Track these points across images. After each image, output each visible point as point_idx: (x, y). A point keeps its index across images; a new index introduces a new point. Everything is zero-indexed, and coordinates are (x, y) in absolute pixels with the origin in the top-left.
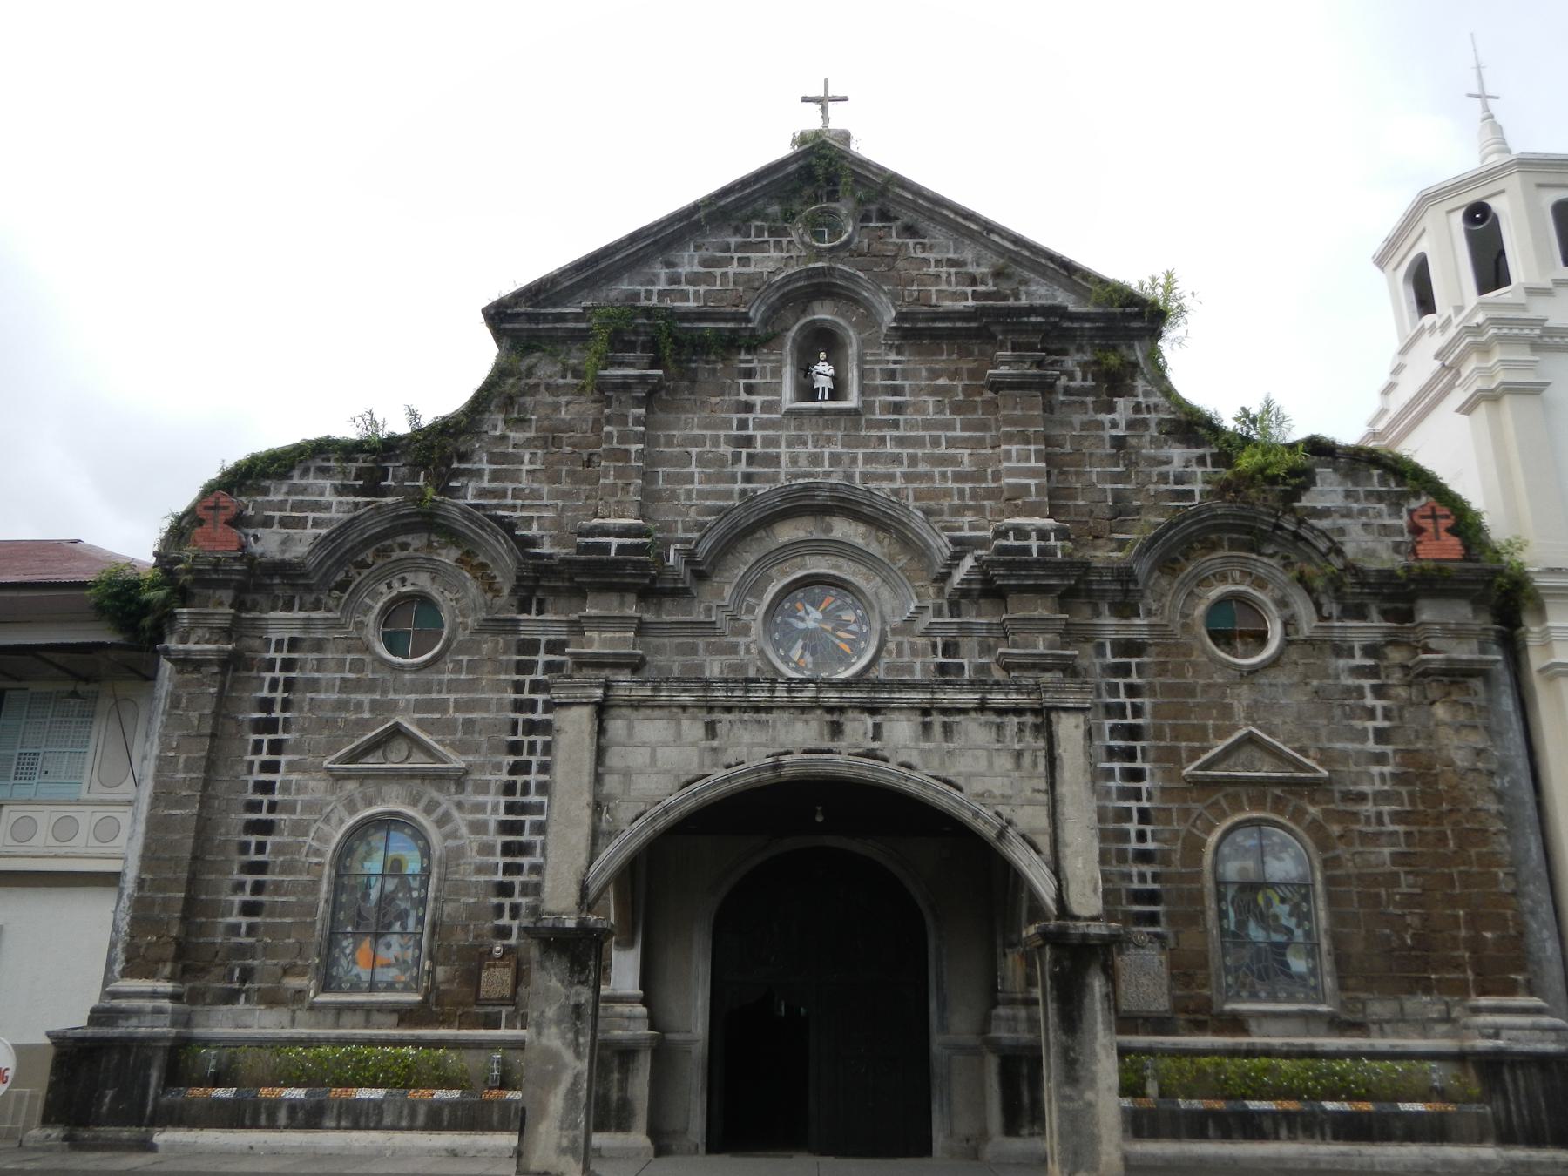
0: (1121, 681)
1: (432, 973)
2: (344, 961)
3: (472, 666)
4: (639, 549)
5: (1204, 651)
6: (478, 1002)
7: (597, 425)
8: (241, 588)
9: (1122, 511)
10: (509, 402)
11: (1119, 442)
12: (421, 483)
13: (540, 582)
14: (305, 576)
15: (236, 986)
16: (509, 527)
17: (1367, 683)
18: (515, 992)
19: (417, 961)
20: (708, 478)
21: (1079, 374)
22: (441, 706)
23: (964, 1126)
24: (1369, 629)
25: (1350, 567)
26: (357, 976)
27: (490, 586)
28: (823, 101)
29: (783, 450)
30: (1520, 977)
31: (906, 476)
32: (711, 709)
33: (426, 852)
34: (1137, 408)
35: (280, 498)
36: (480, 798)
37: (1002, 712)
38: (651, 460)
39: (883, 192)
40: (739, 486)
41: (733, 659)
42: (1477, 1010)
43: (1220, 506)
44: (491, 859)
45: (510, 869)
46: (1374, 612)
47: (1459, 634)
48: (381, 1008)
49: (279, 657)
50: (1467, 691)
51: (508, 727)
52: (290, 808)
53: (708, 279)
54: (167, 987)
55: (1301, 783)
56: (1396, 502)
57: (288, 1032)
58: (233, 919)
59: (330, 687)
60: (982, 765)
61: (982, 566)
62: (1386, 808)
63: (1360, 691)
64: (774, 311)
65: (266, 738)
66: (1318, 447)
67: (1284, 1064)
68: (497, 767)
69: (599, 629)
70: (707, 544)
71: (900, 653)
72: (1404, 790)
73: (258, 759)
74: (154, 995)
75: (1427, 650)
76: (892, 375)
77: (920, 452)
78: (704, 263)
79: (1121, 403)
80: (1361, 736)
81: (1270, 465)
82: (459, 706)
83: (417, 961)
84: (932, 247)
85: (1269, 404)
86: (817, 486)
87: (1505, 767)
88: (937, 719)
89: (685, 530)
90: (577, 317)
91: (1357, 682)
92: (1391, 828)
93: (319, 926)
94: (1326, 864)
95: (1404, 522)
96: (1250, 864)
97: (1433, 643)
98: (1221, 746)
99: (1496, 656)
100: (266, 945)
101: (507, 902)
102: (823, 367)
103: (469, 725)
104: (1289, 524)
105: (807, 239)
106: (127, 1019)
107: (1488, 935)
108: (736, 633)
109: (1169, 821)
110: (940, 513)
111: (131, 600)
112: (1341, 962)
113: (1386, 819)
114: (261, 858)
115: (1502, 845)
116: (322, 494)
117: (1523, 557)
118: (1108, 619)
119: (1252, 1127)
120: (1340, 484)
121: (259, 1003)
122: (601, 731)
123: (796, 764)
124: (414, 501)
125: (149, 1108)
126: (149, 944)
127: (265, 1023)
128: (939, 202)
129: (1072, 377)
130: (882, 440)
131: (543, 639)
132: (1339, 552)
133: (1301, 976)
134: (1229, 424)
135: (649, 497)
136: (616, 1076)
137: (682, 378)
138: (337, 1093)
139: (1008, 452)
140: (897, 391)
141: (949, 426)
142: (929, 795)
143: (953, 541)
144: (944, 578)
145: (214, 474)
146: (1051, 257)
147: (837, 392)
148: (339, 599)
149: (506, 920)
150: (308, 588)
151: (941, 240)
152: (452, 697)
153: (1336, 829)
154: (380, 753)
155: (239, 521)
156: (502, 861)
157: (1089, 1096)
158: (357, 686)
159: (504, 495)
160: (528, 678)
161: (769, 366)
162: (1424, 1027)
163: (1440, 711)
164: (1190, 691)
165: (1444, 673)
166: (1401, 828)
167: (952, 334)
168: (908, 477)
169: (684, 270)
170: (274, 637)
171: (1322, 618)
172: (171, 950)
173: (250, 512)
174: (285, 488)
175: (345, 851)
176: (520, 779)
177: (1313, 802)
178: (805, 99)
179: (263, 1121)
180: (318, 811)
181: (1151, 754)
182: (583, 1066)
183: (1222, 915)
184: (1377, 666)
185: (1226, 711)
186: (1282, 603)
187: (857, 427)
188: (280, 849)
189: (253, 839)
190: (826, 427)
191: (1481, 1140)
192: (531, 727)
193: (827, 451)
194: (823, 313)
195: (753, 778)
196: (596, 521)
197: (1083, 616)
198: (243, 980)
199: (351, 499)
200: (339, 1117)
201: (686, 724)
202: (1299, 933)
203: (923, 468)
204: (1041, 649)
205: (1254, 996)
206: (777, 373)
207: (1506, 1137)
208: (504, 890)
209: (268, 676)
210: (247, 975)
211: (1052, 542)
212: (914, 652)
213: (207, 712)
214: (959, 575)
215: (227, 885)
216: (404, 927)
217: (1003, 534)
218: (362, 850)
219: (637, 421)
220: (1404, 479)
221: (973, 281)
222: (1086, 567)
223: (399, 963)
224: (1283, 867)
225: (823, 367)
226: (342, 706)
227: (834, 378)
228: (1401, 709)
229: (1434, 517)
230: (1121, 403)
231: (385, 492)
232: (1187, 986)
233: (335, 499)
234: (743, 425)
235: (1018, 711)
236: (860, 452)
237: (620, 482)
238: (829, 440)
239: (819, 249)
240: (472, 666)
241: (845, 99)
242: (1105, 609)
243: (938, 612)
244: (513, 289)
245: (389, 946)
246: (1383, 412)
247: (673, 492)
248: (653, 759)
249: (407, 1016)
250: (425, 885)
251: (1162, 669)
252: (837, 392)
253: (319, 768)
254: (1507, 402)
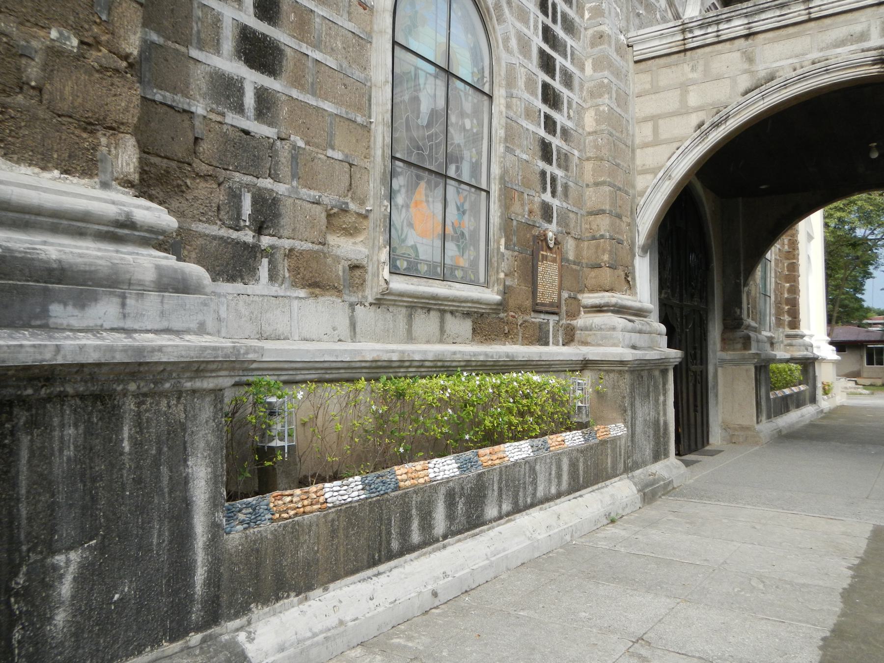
15: (247, 236)
26: (415, 248)
54: (151, 213)
74: (121, 231)
106: (82, 301)
121: (294, 285)
125: (200, 575)
126: (55, 52)
136: (662, 398)
198: (260, 230)
249: (486, 322)
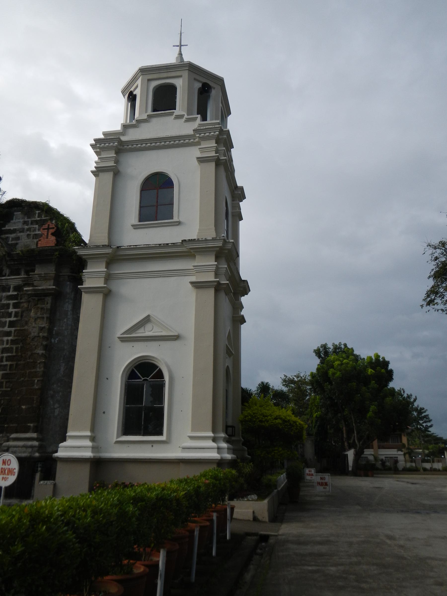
17: (11, 302)
30: (32, 425)
46: (23, 273)
47: (45, 278)
56: (41, 223)
62: (5, 355)
72: (14, 347)
91: (8, 302)
92: (5, 363)
99: (68, 289)
107: (24, 407)
113: (4, 359)
120: (23, 218)
165: (36, 295)
166: (9, 363)
184: (18, 294)
228: (23, 312)
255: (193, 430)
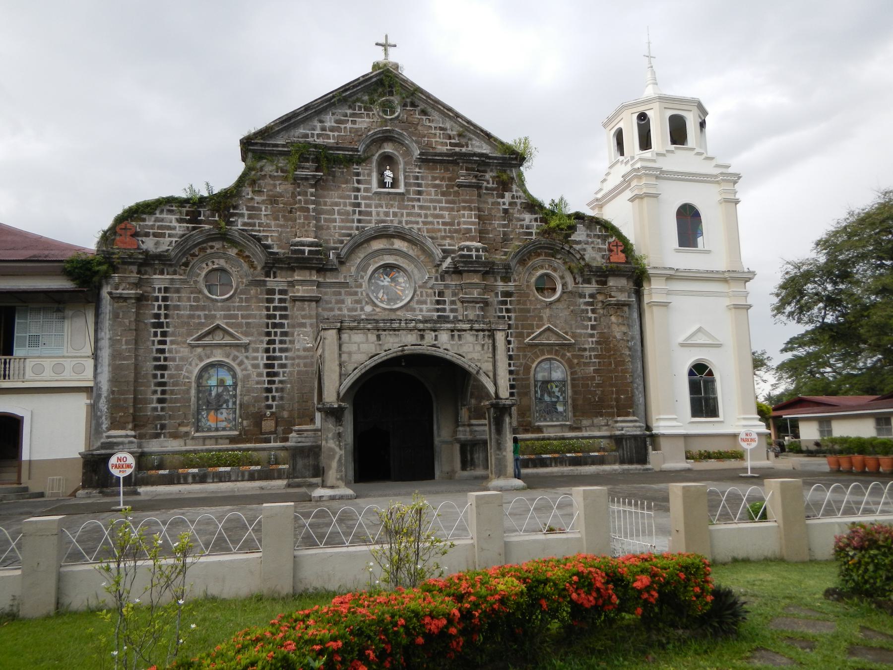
0: (504, 307)
1: (242, 423)
2: (203, 420)
3: (247, 300)
4: (317, 252)
5: (534, 296)
6: (262, 433)
7: (294, 196)
8: (140, 265)
9: (506, 239)
10: (253, 183)
11: (506, 211)
12: (217, 219)
13: (275, 264)
14: (170, 260)
16: (259, 240)
17: (589, 308)
18: (276, 430)
19: (235, 419)
20: (342, 221)
21: (491, 182)
22: (235, 317)
23: (446, 468)
24: (590, 288)
25: (588, 265)
27: (252, 266)
28: (385, 46)
29: (373, 209)
31: (423, 222)
32: (378, 330)
33: (234, 376)
34: (513, 197)
35: (151, 223)
36: (255, 354)
37: (477, 330)
38: (319, 212)
39: (413, 94)
40: (356, 224)
41: (356, 298)
42: (617, 422)
43: (543, 240)
44: (263, 379)
45: (269, 382)
47: (621, 290)
48: (222, 437)
49: (160, 295)
50: (623, 311)
51: (265, 326)
52: (174, 359)
53: (338, 129)
54: (133, 433)
55: (565, 345)
56: (604, 239)
57: (184, 448)
58: (154, 405)
59: (185, 309)
60: (471, 349)
61: (454, 262)
62: (593, 354)
63: (587, 310)
64: (368, 146)
65: (159, 330)
66: (579, 216)
67: (555, 442)
68: (262, 342)
69: (301, 285)
70: (345, 250)
71: (422, 296)
72: (599, 347)
73: (156, 339)
74: (127, 436)
75: (611, 296)
76: (417, 178)
77: (429, 212)
78: (337, 122)
79: (507, 194)
80: (586, 327)
81: (561, 224)
82: (243, 317)
83: (235, 419)
84: (433, 121)
85: (562, 199)
86: (389, 227)
87: (633, 338)
88: (456, 333)
89: (334, 243)
90: (283, 146)
93: (192, 407)
94: (572, 373)
95: (606, 247)
96: (546, 374)
97: (613, 294)
98: (538, 331)
100: (170, 415)
101: (270, 395)
102: (388, 173)
103: (248, 324)
104: (567, 248)
105: (381, 114)
108: (357, 287)
109: (519, 359)
110: (437, 238)
111: (90, 270)
112: (575, 407)
114: (163, 380)
115: (630, 366)
116: (171, 222)
117: (645, 262)
118: (500, 283)
119: (543, 463)
122: (340, 338)
123: (409, 350)
124: (218, 228)
126: (121, 417)
127: (173, 445)
128: (437, 102)
129: (488, 183)
130: (413, 207)
131: (277, 289)
132: (584, 259)
133: (561, 412)
134: (547, 206)
135: (318, 228)
137: (329, 175)
138: (210, 469)
139: (464, 215)
140: (419, 185)
141: (440, 202)
142: (454, 360)
143: (444, 251)
144: (439, 265)
145: (119, 211)
146: (482, 131)
147: (394, 184)
148: (185, 270)
149: (270, 402)
150: (171, 265)
151: (437, 117)
152: (240, 313)
153: (576, 361)
154: (211, 336)
155: (135, 235)
156: (266, 379)
157: (504, 453)
158: (197, 308)
159: (254, 225)
160: (272, 305)
161: (366, 171)
162: (599, 428)
163: (613, 319)
164: (528, 311)
165: (616, 305)
166: (597, 360)
167: (441, 162)
168: (425, 223)
169: (327, 124)
170: (157, 287)
171: (576, 283)
172: (131, 418)
173: (138, 230)
174: (153, 219)
175: (200, 376)
176: (272, 347)
177: (569, 352)
178: (377, 44)
179: (182, 481)
180: (187, 362)
181: (514, 335)
182: (342, 452)
183: (536, 392)
185: (541, 318)
186: (562, 278)
187: (403, 200)
188: (171, 376)
189: (159, 373)
190: (391, 200)
191: (614, 463)
192: (275, 325)
193: (391, 210)
194: (388, 148)
195: (394, 355)
196: (297, 239)
197: (490, 281)
199: (185, 225)
200: (213, 478)
201: (370, 335)
202: (561, 398)
203: (430, 219)
204: (476, 296)
205: (545, 420)
206: (369, 175)
207: (622, 462)
208: (269, 390)
209: (156, 304)
210: (163, 427)
211: (481, 253)
212: (427, 295)
213: (132, 319)
214: (445, 265)
215: (149, 392)
216: (228, 406)
217: (461, 249)
218: (206, 376)
219: (312, 195)
220: (608, 229)
221: (450, 138)
222: (493, 263)
223: (226, 420)
224: (557, 375)
225: (388, 173)
226: (191, 317)
227: (393, 179)
229: (617, 246)
230: (507, 194)
231: (201, 222)
232: (523, 417)
233: (177, 225)
234: (356, 197)
235: (483, 330)
236: (405, 211)
237: (306, 222)
238: (392, 206)
239: (386, 119)
240: (247, 300)
241: (395, 46)
242: (499, 279)
243: (436, 280)
244: (253, 131)
245: (222, 413)
246: (601, 190)
247: (328, 226)
248: (359, 349)
250: (235, 389)
251: (519, 302)
252: (394, 184)
253: (184, 343)
254: (646, 199)
255: (745, 413)
